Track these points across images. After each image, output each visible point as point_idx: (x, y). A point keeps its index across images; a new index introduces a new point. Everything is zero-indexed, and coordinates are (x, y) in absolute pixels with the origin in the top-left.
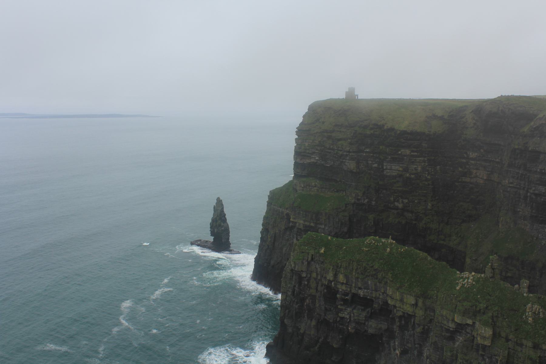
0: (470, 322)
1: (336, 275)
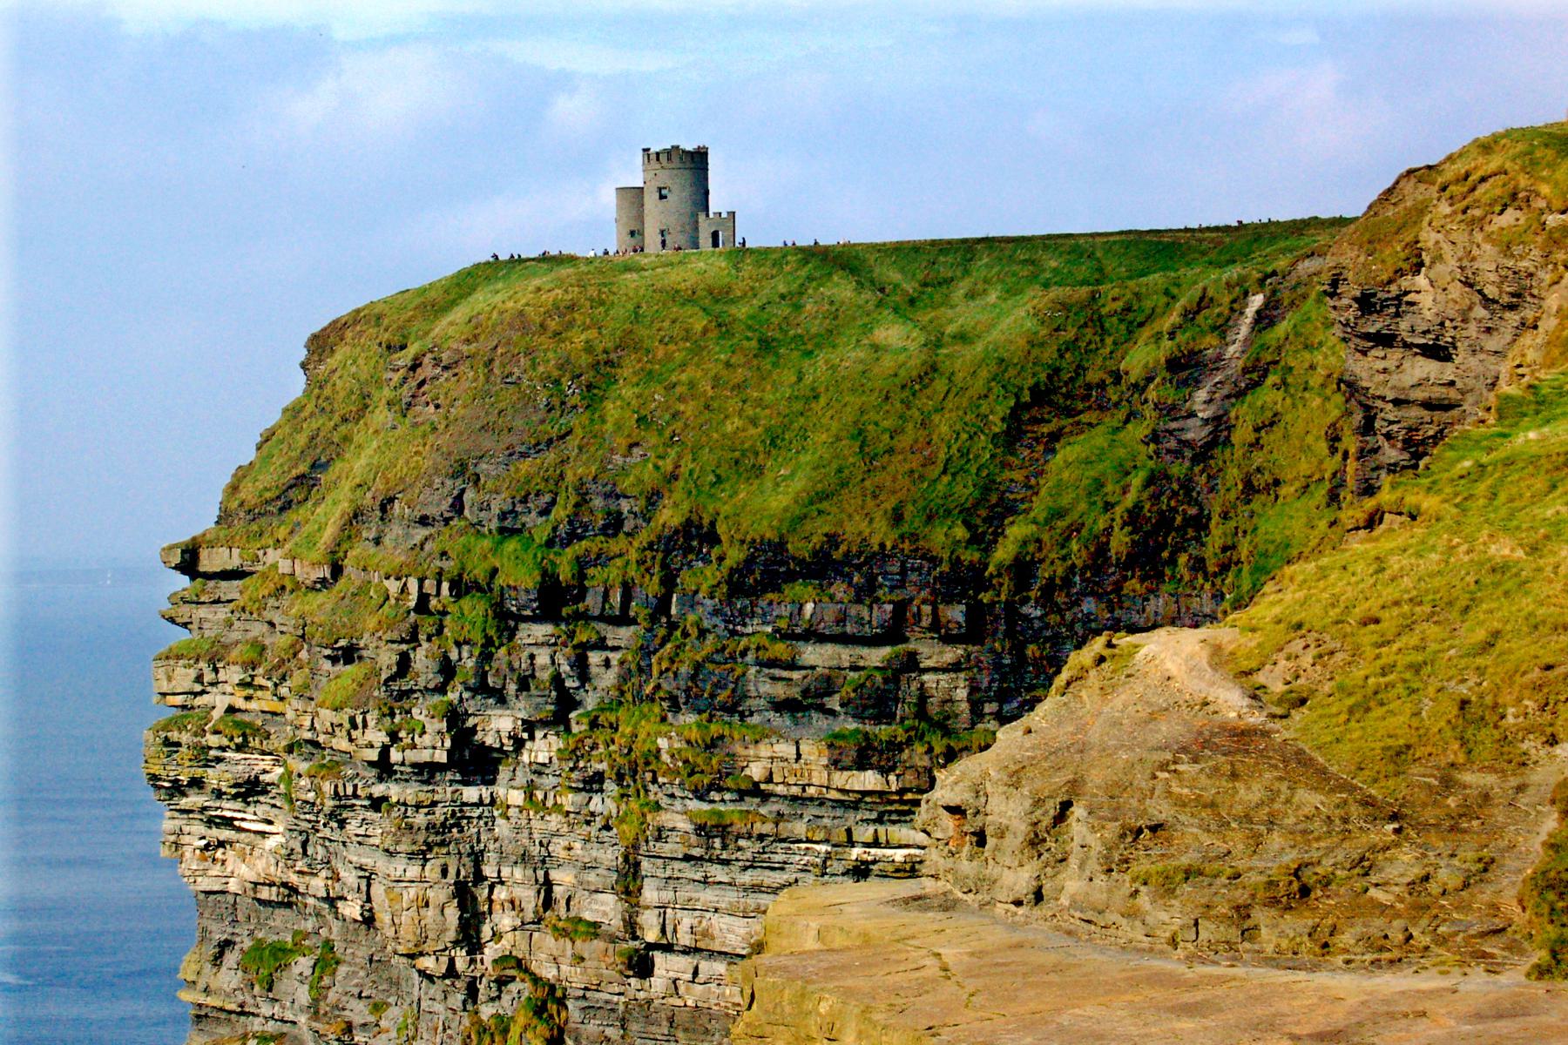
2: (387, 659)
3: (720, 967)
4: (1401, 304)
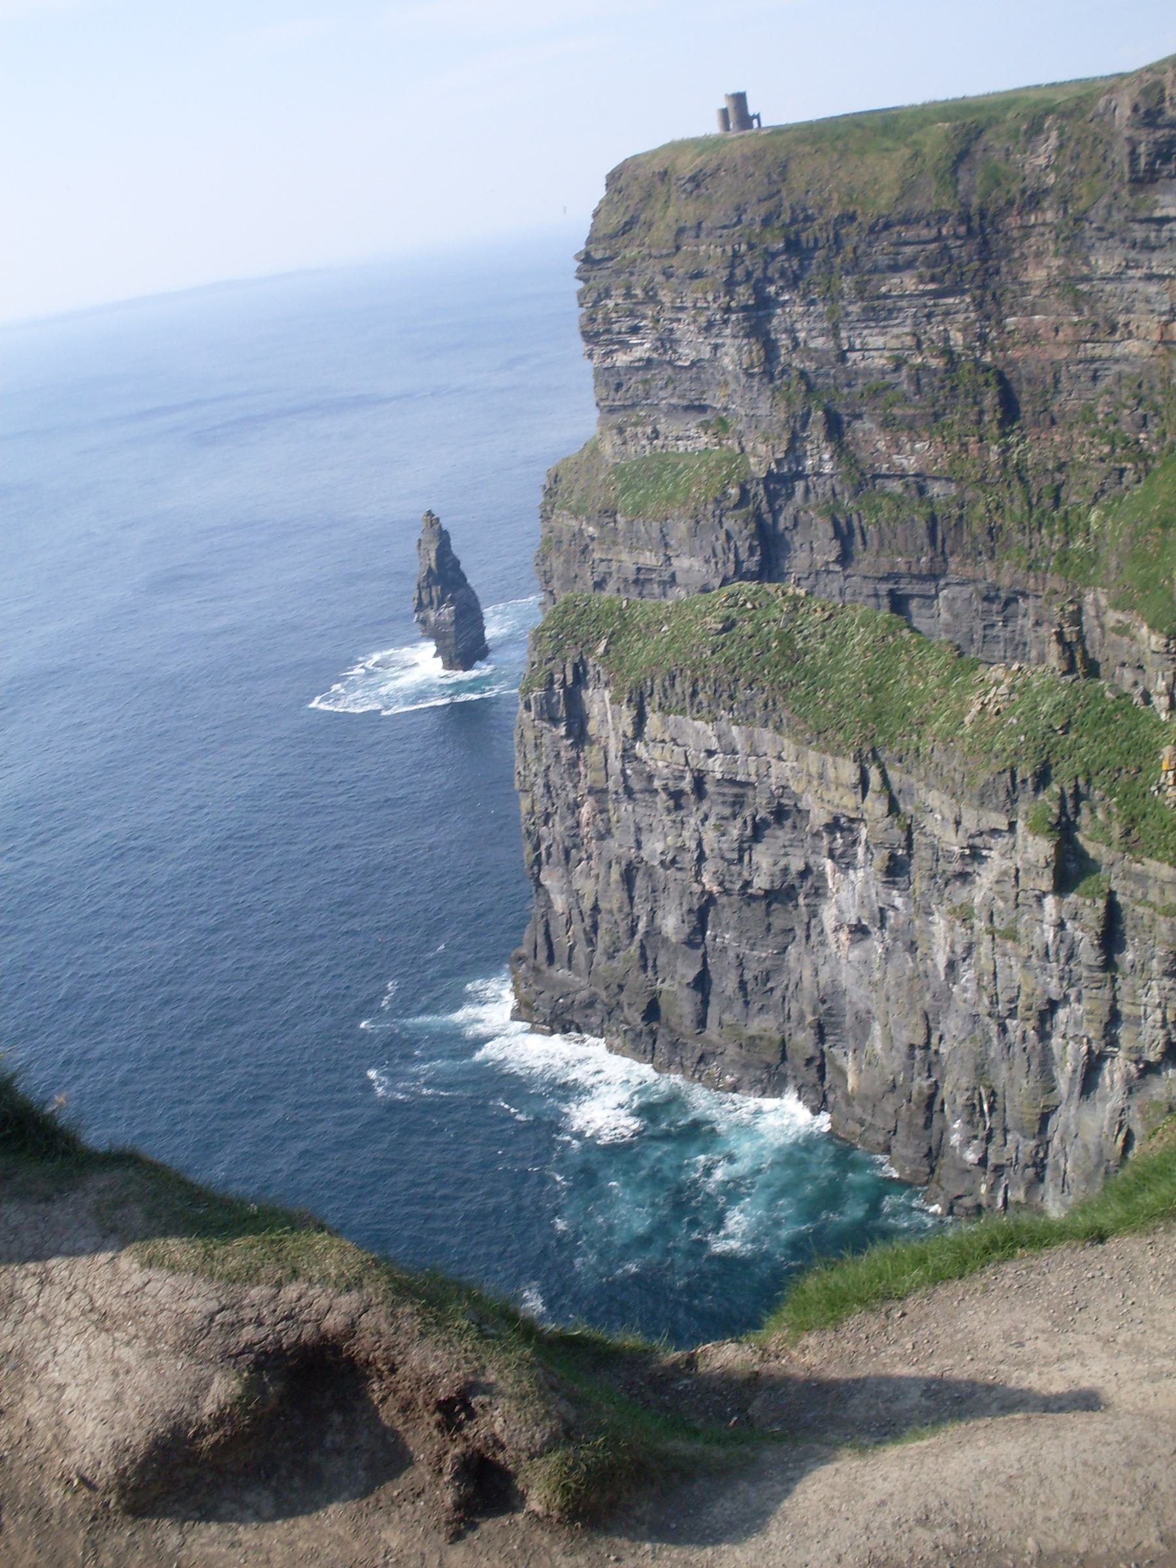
0: (1002, 823)
1: (640, 721)
2: (724, 274)
3: (873, 353)
4: (1161, 112)
